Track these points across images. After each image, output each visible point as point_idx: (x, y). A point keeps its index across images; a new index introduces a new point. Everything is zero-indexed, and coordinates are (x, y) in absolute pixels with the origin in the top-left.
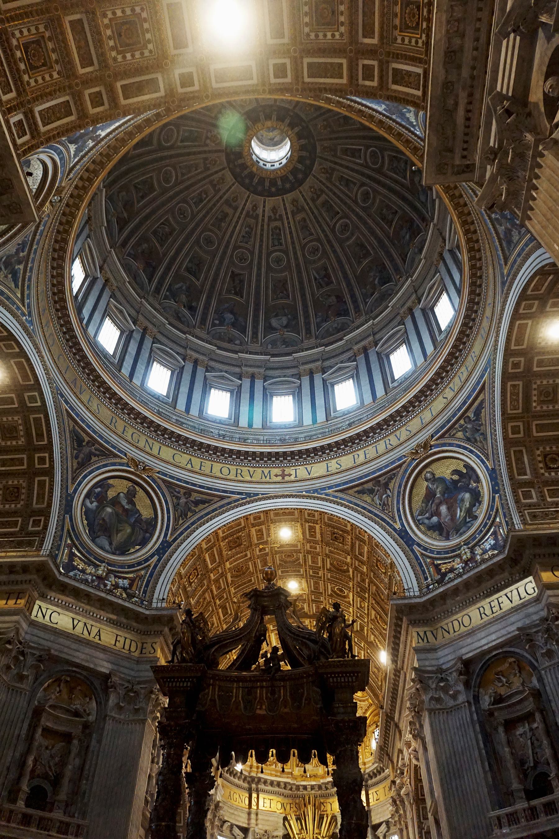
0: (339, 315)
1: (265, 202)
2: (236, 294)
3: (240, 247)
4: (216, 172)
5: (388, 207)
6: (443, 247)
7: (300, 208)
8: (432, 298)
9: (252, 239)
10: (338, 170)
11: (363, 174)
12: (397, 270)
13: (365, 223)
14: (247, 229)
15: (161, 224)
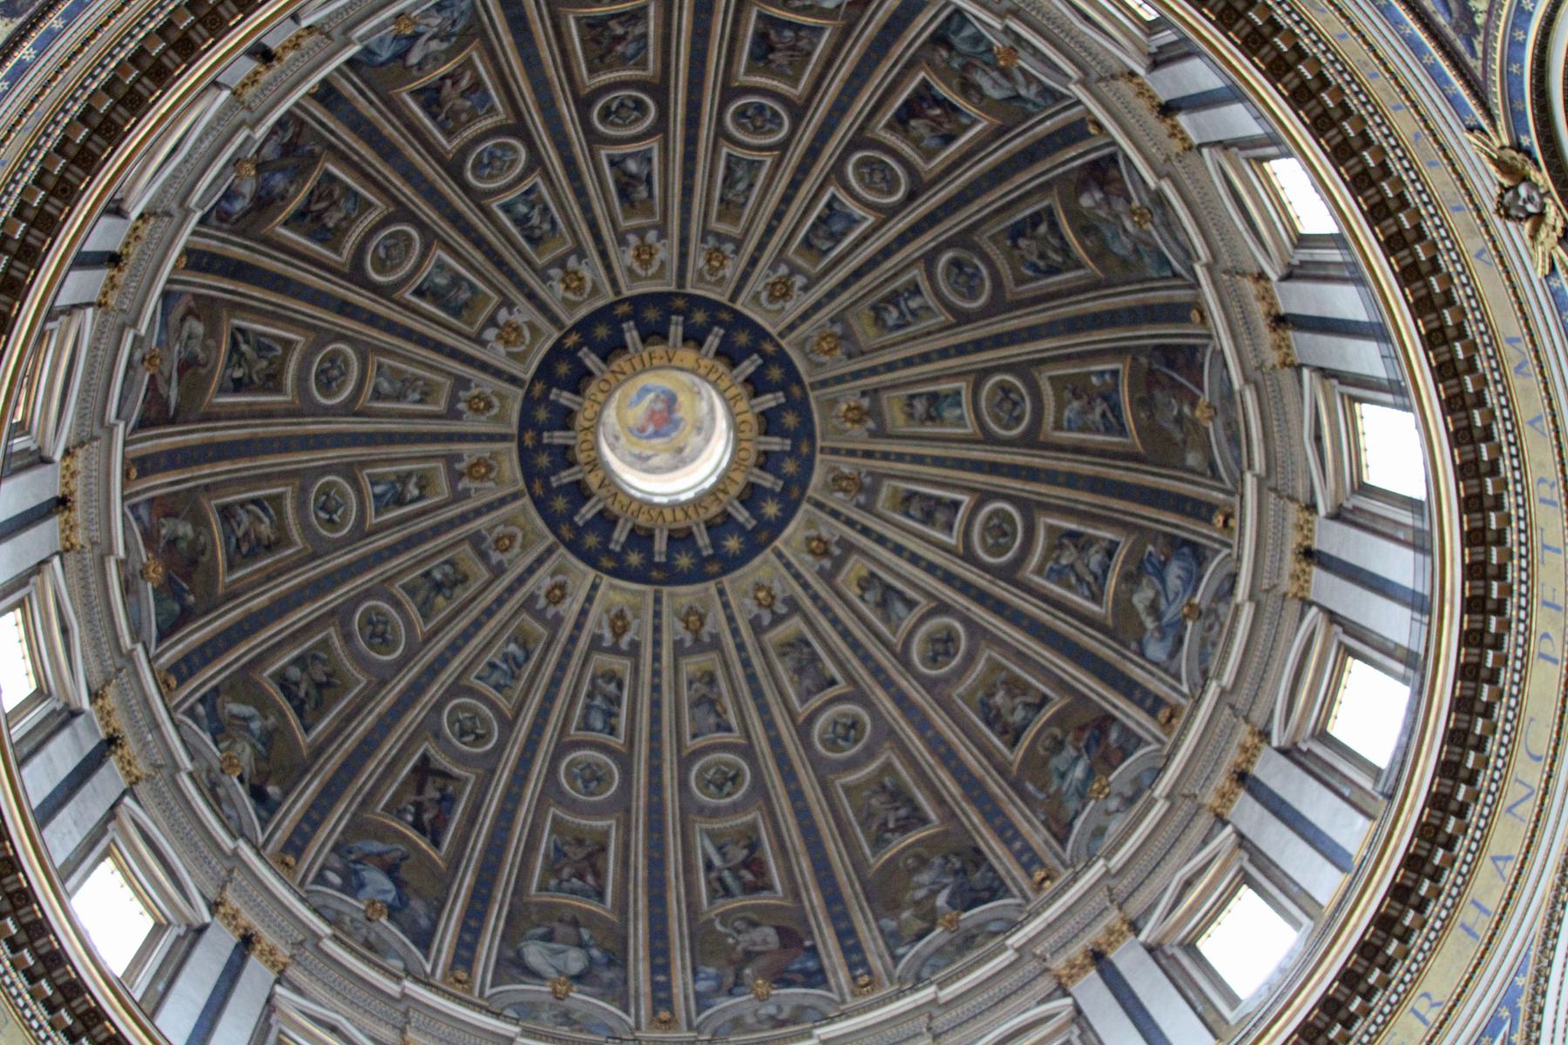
0: (782, 979)
1: (594, 587)
2: (418, 825)
3: (471, 692)
4: (477, 438)
5: (1015, 686)
6: (1250, 753)
7: (706, 639)
8: (1193, 909)
9: (522, 683)
10: (864, 553)
11: (948, 578)
12: (1029, 859)
13: (922, 725)
14: (513, 648)
15: (256, 501)
